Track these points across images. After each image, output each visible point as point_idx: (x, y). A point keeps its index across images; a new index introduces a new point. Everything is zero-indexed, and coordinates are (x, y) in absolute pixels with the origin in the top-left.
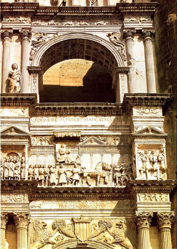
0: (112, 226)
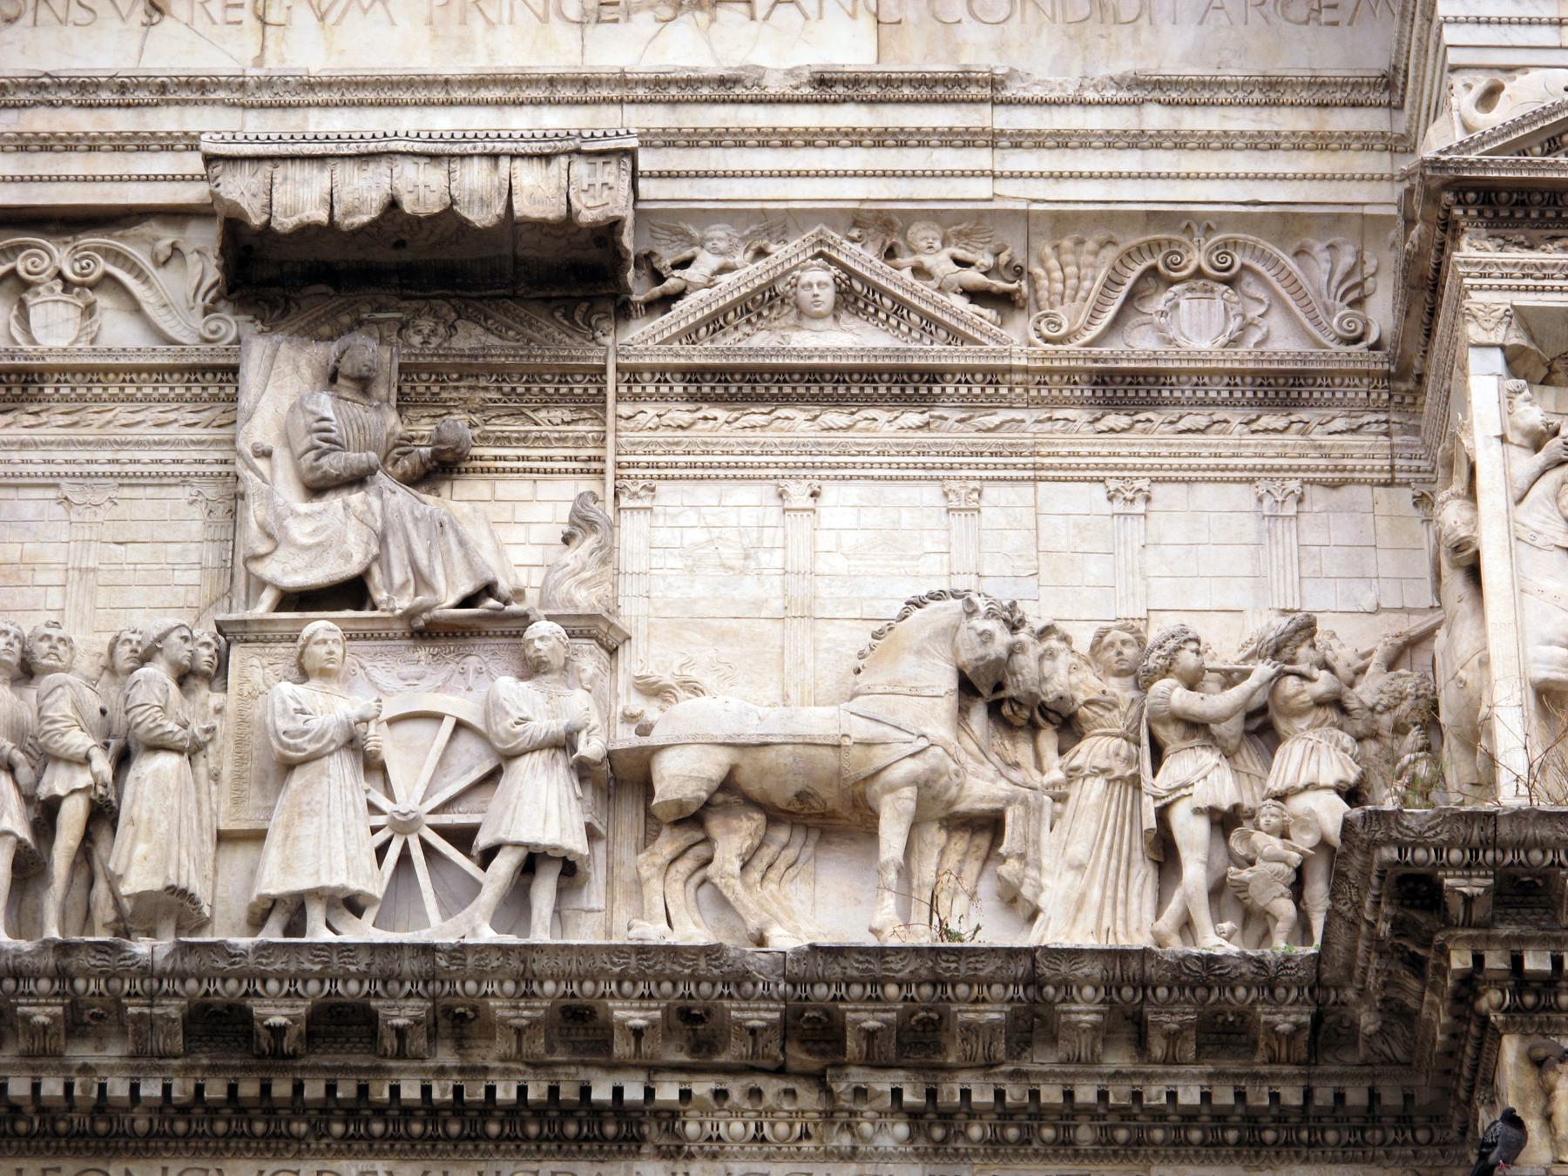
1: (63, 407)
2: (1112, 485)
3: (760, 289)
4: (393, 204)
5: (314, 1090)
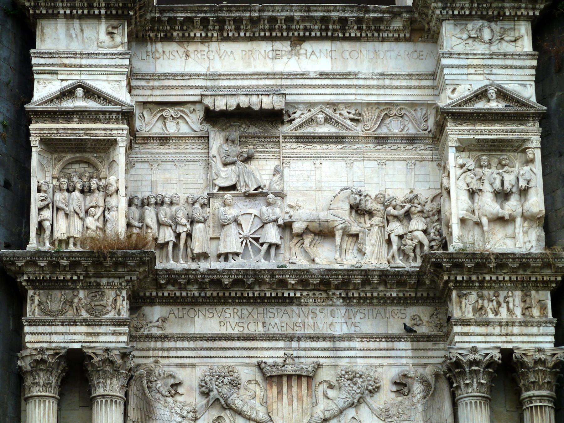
0: (378, 388)
1: (174, 144)
2: (379, 161)
3: (310, 119)
4: (238, 105)
5: (233, 294)
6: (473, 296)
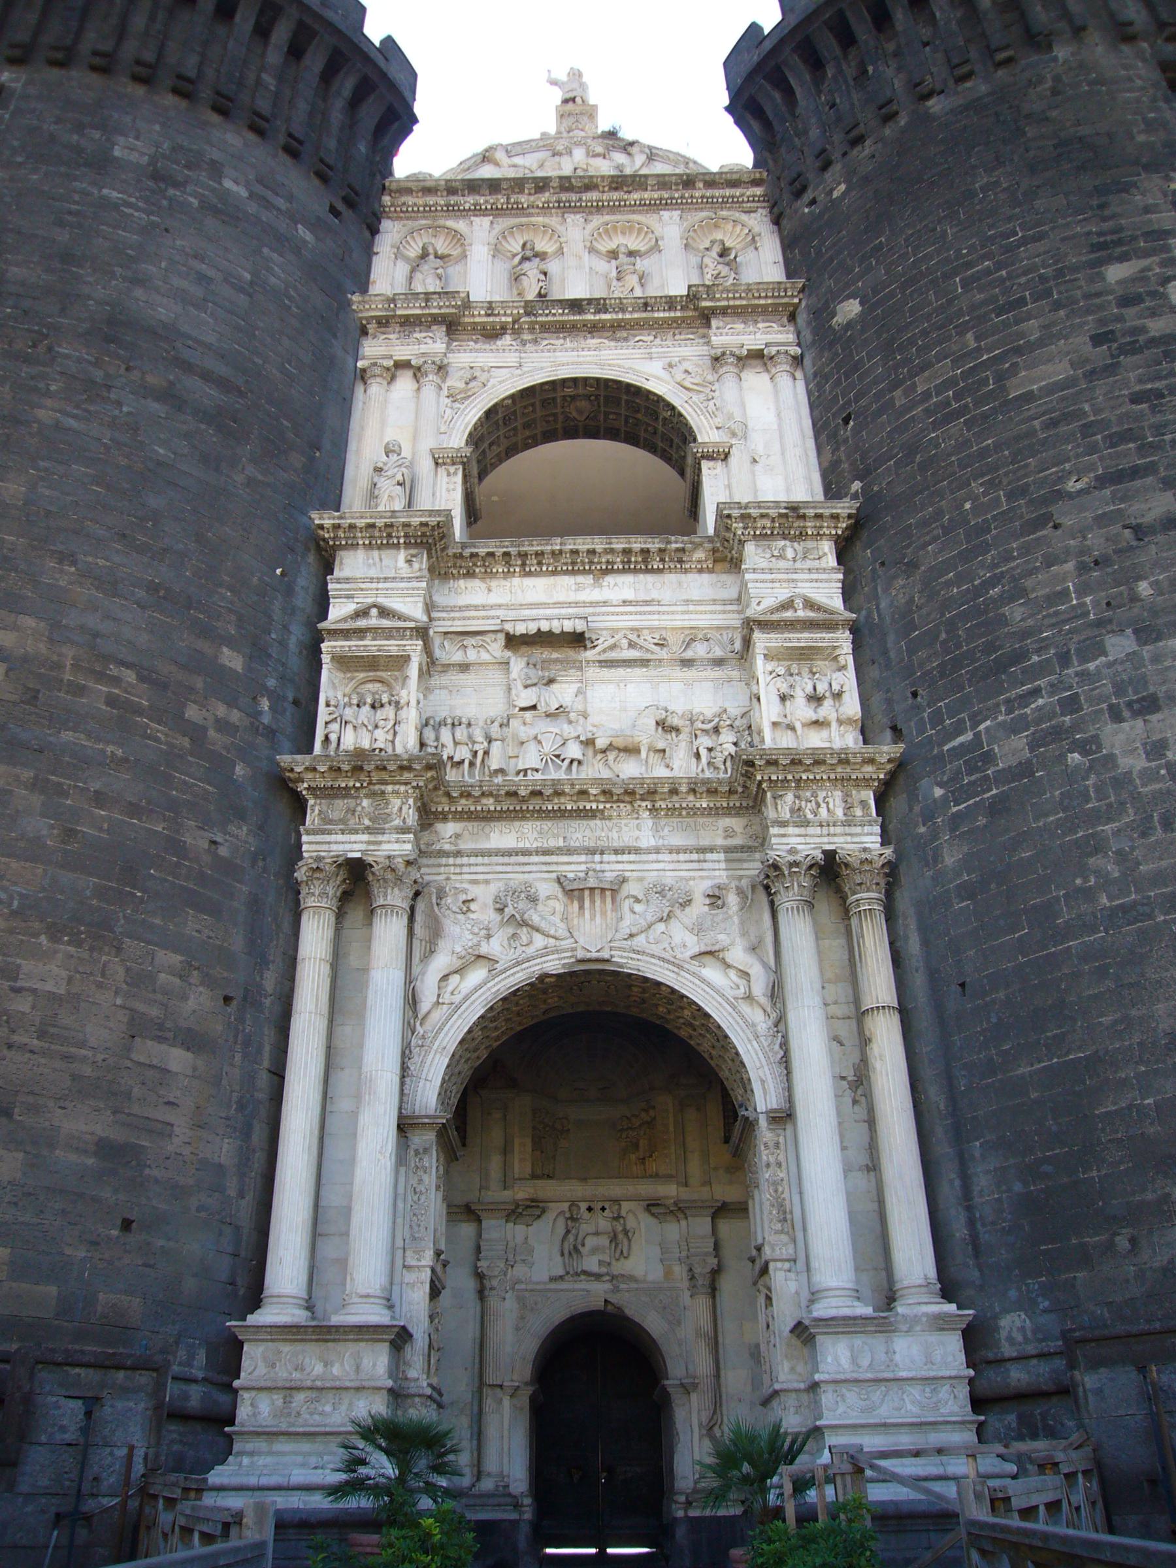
0: (690, 901)
5: (531, 808)
6: (790, 797)
